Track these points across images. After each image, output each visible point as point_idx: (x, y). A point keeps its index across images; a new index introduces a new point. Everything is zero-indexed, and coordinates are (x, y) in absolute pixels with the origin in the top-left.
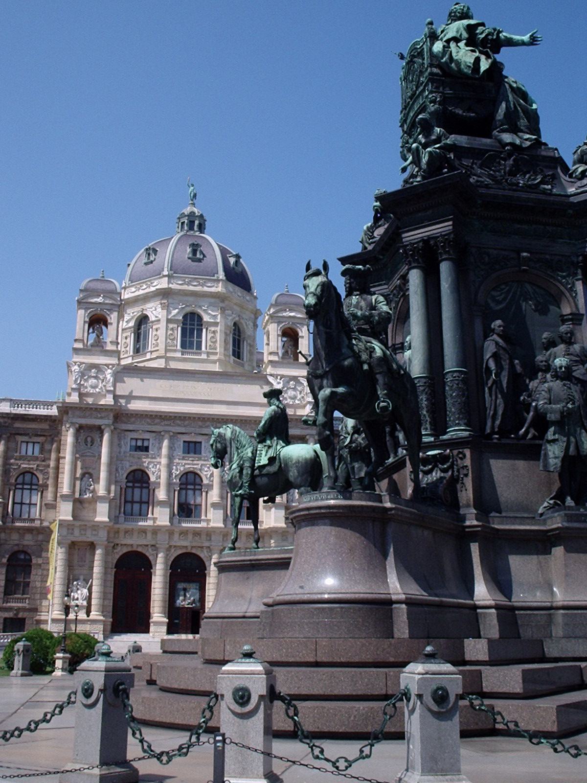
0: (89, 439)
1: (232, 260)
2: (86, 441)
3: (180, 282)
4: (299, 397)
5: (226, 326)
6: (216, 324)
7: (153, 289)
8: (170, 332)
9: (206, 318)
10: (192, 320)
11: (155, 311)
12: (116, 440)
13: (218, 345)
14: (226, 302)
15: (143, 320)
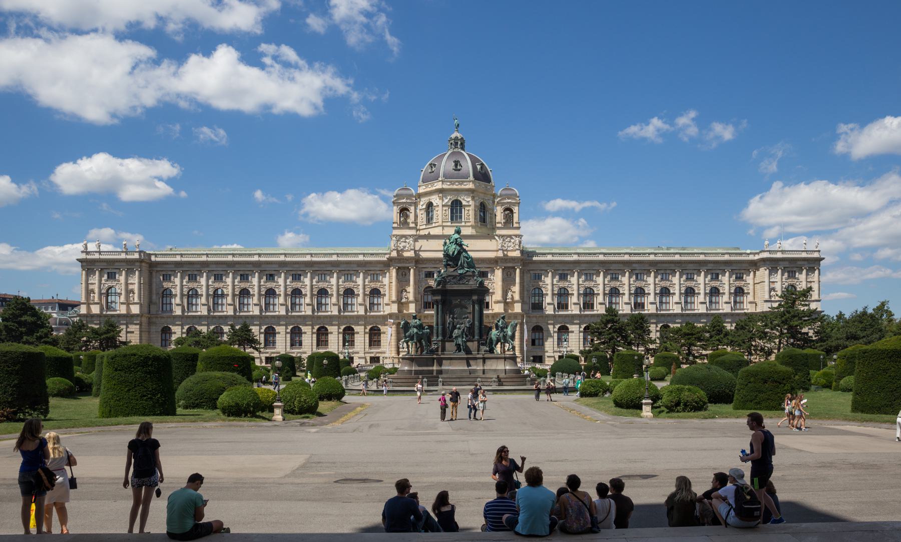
0: (404, 273)
1: (479, 167)
2: (402, 274)
3: (448, 184)
4: (513, 246)
5: (475, 206)
6: (469, 206)
7: (434, 188)
8: (444, 212)
9: (464, 203)
10: (457, 204)
11: (436, 200)
12: (417, 273)
13: (470, 217)
14: (475, 193)
15: (430, 205)
